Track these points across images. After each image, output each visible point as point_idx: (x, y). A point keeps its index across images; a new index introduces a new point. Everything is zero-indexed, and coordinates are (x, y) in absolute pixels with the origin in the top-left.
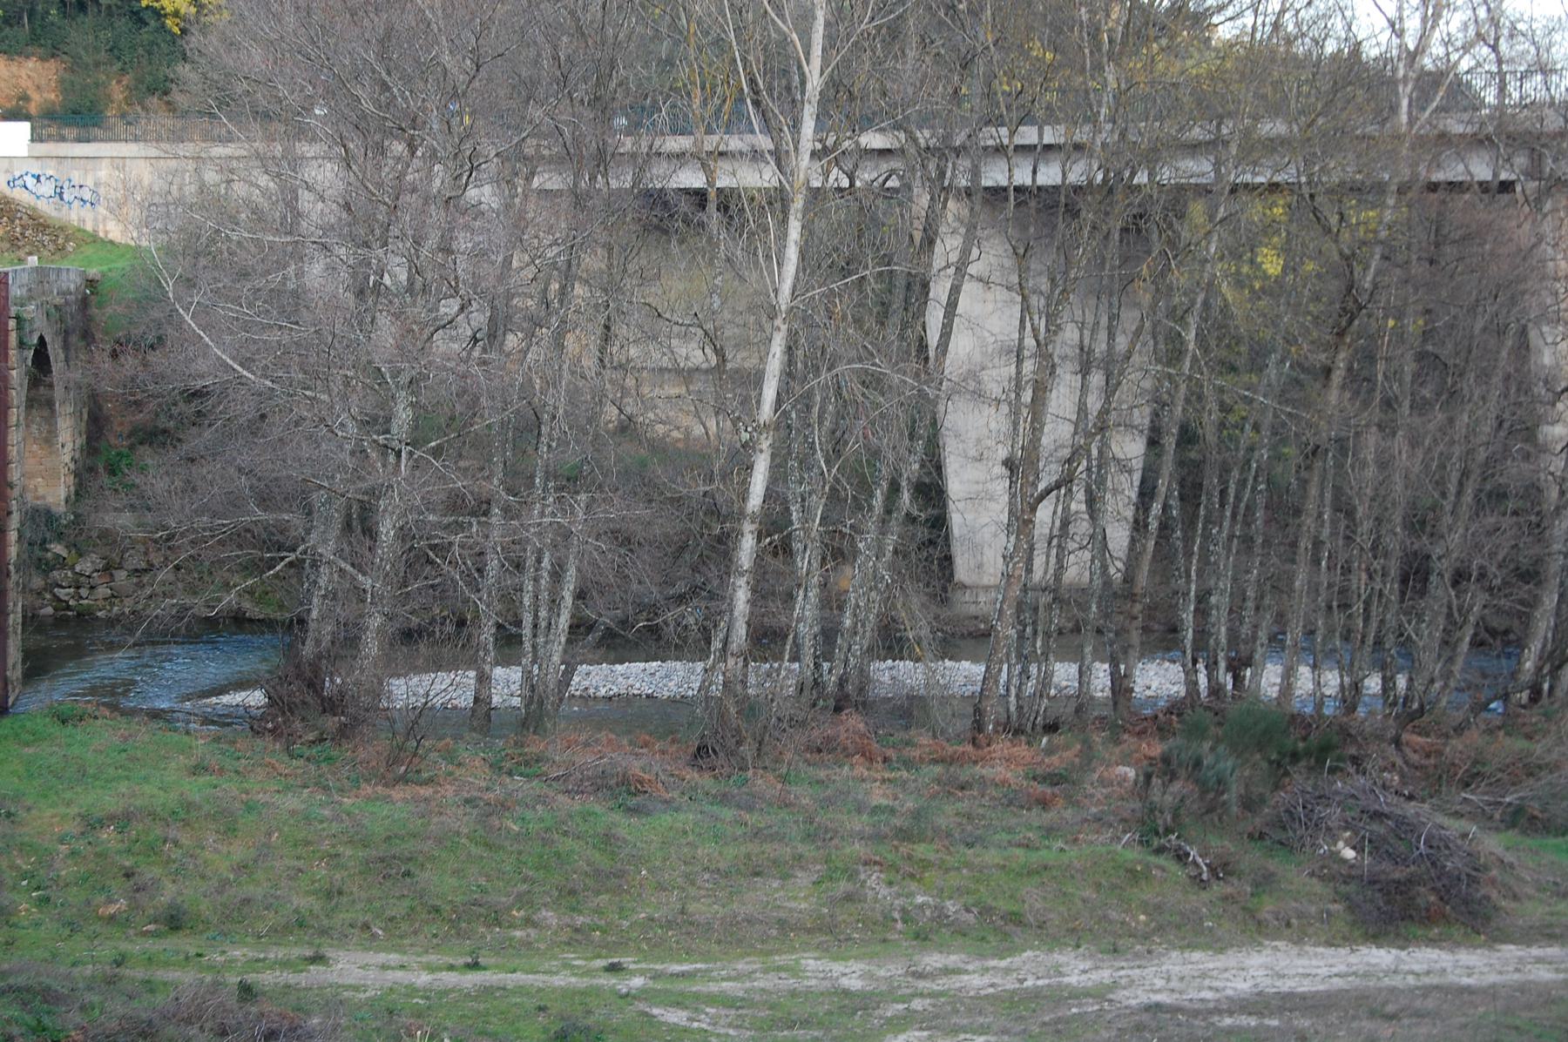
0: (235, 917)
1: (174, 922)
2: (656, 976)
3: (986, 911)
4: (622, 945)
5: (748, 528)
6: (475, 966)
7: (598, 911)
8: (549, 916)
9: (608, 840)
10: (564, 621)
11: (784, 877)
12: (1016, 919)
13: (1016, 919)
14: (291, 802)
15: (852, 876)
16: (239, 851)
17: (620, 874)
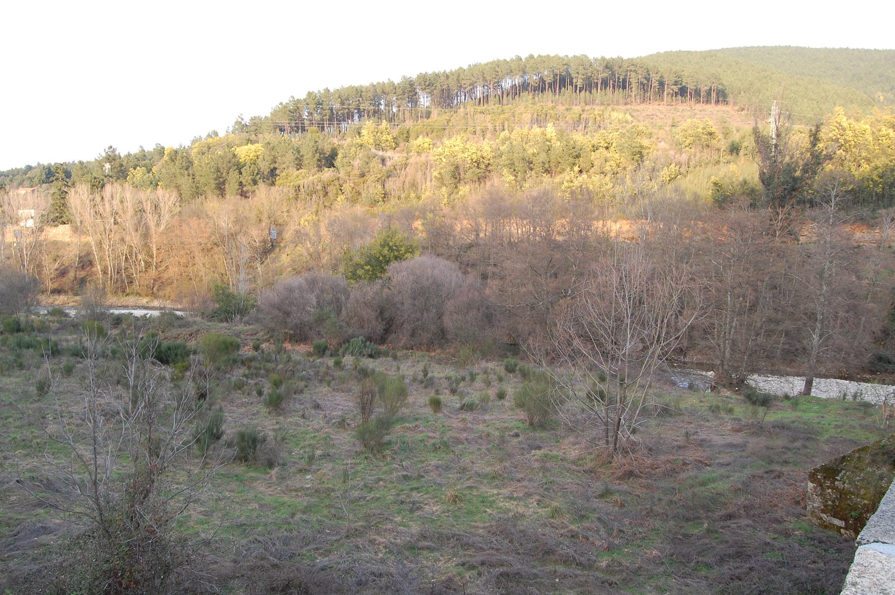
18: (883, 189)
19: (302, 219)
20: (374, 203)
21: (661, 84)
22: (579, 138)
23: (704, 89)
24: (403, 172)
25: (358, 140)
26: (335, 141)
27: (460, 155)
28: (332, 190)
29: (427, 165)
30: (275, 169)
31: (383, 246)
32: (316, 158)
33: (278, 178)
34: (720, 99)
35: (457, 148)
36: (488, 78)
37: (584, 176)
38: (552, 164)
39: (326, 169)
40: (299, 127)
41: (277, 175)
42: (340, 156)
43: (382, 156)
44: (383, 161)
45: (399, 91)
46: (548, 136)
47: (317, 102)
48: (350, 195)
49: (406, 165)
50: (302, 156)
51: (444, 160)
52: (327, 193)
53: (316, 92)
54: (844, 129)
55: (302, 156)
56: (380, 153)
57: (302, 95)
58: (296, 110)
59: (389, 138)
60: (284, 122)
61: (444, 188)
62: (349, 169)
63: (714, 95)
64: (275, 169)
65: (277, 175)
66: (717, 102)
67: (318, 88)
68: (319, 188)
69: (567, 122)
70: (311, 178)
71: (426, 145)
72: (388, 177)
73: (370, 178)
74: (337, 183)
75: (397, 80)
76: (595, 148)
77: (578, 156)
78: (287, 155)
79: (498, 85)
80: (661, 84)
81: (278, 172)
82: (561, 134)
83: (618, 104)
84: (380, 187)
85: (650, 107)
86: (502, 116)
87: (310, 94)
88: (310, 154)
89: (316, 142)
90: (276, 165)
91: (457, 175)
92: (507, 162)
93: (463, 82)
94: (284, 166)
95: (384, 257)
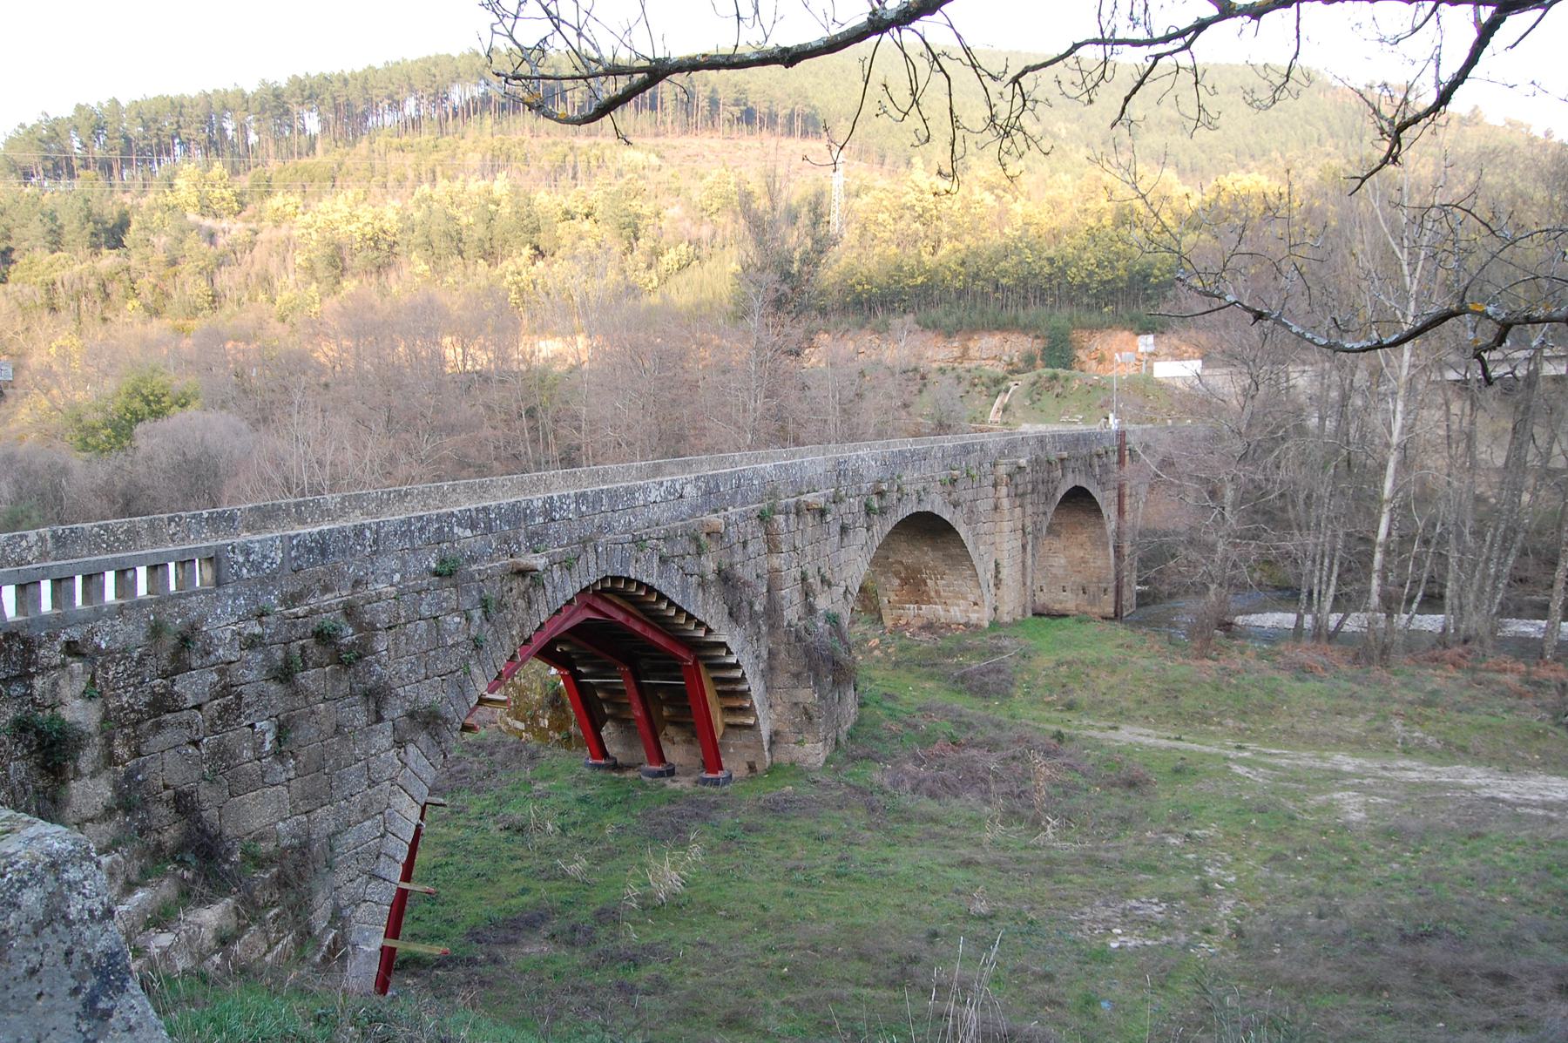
0: (1095, 707)
1: (1070, 707)
2: (1259, 753)
3: (1447, 743)
4: (1250, 739)
5: (1378, 549)
6: (1179, 739)
7: (1254, 723)
8: (1230, 722)
9: (1273, 692)
10: (1332, 591)
11: (1353, 717)
12: (1463, 749)
13: (1463, 749)
14: (1146, 662)
15: (1385, 718)
16: (1114, 680)
17: (1273, 707)
18: (965, 282)
19: (54, 344)
20: (195, 311)
21: (714, 103)
22: (545, 200)
23: (783, 113)
24: (247, 257)
25: (171, 200)
26: (127, 199)
27: (343, 228)
28: (116, 289)
29: (288, 244)
30: (11, 250)
31: (131, 396)
32: (87, 232)
33: (12, 268)
34: (810, 129)
35: (337, 216)
36: (418, 86)
37: (540, 264)
38: (495, 243)
39: (105, 251)
40: (61, 167)
41: (13, 262)
42: (134, 226)
43: (210, 228)
44: (211, 237)
45: (255, 106)
46: (496, 195)
47: (96, 124)
48: (150, 299)
49: (253, 244)
50: (61, 227)
51: (315, 236)
52: (108, 295)
53: (94, 105)
54: (922, 192)
55: (61, 227)
56: (208, 222)
57: (67, 111)
58: (52, 139)
59: (227, 194)
60: (31, 158)
61: (314, 285)
62: (148, 250)
63: (798, 123)
64: (11, 250)
65: (13, 262)
66: (805, 134)
67: (97, 97)
68: (92, 285)
69: (540, 168)
70: (77, 268)
71: (290, 209)
72: (219, 266)
73: (187, 268)
74: (125, 277)
75: (251, 87)
76: (568, 215)
77: (537, 229)
78: (31, 226)
79: (440, 97)
80: (714, 103)
81: (15, 256)
82: (515, 190)
83: (643, 135)
84: (204, 284)
85: (696, 141)
86: (435, 156)
87: (79, 108)
88: (76, 224)
89: (87, 201)
90: (12, 244)
91: (337, 261)
92: (421, 240)
93: (375, 92)
94: (26, 244)
95: (134, 413)
